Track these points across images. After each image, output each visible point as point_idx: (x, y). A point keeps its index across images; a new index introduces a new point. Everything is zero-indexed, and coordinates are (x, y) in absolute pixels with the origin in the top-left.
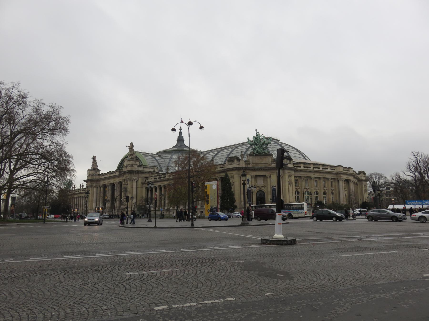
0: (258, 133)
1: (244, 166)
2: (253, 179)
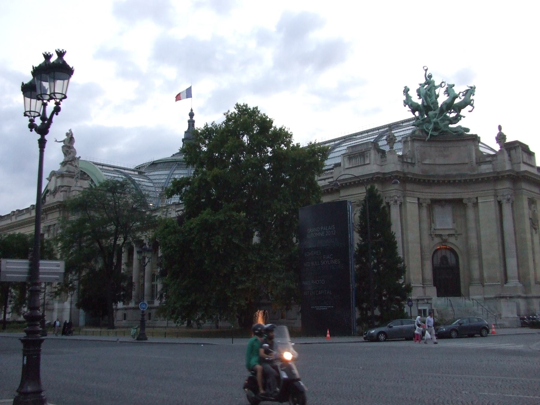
0: (430, 76)
1: (398, 168)
2: (425, 212)
